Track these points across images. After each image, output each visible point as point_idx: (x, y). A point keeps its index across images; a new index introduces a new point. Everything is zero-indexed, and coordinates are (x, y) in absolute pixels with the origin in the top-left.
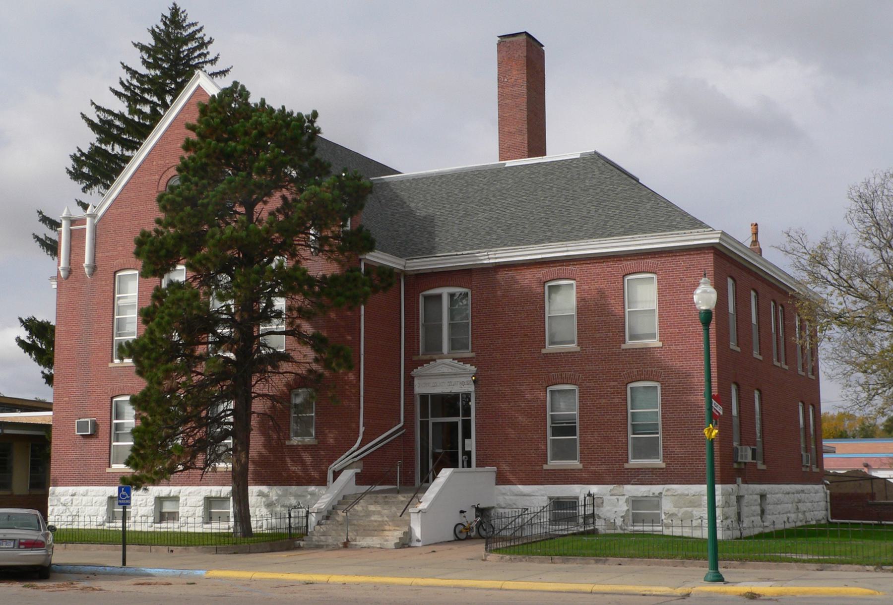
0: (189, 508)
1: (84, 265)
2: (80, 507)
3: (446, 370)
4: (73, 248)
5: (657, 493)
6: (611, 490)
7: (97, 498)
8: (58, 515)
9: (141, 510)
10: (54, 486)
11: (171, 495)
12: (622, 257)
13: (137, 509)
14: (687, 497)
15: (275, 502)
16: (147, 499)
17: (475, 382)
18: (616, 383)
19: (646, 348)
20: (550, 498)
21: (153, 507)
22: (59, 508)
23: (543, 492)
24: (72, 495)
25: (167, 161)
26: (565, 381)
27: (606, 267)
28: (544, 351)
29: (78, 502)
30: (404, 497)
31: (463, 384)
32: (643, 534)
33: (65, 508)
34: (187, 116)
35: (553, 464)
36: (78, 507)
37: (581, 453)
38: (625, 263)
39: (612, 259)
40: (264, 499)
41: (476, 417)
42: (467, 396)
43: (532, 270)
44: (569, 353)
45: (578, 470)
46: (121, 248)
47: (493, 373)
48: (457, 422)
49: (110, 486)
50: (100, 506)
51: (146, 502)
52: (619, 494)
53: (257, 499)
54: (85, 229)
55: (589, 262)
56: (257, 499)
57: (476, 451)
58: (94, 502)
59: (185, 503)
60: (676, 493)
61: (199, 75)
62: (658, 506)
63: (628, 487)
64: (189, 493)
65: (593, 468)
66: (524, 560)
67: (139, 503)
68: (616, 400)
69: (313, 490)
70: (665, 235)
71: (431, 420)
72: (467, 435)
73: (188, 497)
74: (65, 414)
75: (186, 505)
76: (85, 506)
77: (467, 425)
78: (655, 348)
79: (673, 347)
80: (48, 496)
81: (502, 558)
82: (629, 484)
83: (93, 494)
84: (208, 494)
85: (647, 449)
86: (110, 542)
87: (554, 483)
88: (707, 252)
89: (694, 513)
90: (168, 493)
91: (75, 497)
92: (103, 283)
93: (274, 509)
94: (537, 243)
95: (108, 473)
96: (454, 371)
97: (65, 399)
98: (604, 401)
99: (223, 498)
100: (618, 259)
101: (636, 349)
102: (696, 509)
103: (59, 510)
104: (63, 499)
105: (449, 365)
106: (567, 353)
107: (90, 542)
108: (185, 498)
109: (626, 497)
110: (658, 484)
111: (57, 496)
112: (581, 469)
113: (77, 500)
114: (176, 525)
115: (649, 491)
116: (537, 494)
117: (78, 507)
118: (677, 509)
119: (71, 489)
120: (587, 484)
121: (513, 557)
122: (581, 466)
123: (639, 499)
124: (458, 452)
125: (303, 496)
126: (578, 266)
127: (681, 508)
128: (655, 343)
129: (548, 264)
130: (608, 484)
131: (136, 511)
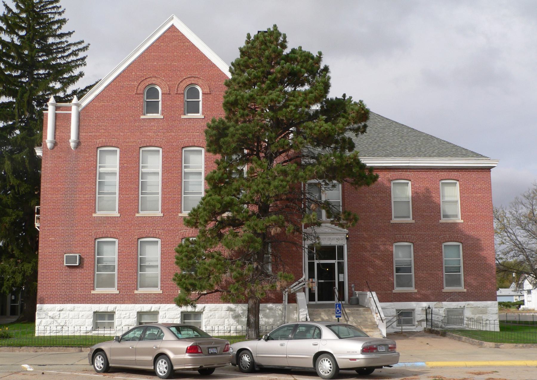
0: (168, 319)
1: (70, 141)
2: (67, 320)
3: (327, 230)
4: (57, 127)
5: (462, 306)
6: (435, 305)
7: (83, 312)
8: (46, 326)
9: (125, 321)
10: (40, 304)
11: (152, 310)
12: (439, 170)
13: (121, 321)
14: (479, 308)
15: (241, 314)
16: (130, 313)
17: (347, 239)
18: (436, 243)
19: (454, 223)
20: (397, 310)
21: (136, 319)
22: (47, 320)
23: (393, 307)
24: (60, 311)
25: (145, 73)
26: (406, 240)
27: (431, 175)
28: (392, 222)
29: (65, 315)
30: (350, 310)
31: (338, 239)
32: (454, 330)
33: (53, 320)
34: (162, 44)
35: (397, 290)
36: (65, 320)
37: (416, 283)
38: (441, 173)
39: (433, 170)
40: (231, 313)
41: (348, 260)
42: (341, 248)
43: (383, 172)
44: (408, 223)
45: (414, 293)
46: (103, 131)
47: (359, 233)
48: (334, 263)
49: (95, 304)
50: (86, 318)
51: (130, 315)
52: (439, 307)
53: (226, 313)
54: (70, 115)
55: (419, 171)
56: (226, 313)
57: (348, 281)
58: (80, 316)
59: (164, 316)
60: (473, 306)
61: (173, 18)
62: (462, 313)
63: (445, 303)
64: (168, 309)
65: (423, 292)
66: (532, 347)
67: (122, 316)
68: (437, 252)
69: (271, 306)
70: (479, 159)
71: (316, 262)
72: (341, 271)
73: (167, 312)
74: (51, 250)
75: (165, 317)
76: (72, 318)
77: (341, 265)
78: (459, 223)
79: (469, 223)
80: (35, 311)
81: (516, 346)
82: (445, 301)
83: (80, 309)
84: (139, 310)
85: (455, 281)
86: (59, 345)
87: (400, 301)
88: (487, 171)
89: (484, 317)
90: (149, 309)
91: (62, 312)
92: (87, 155)
93: (240, 319)
94: (386, 156)
95: (92, 294)
96: (340, 232)
97: (50, 239)
98: (429, 253)
99: (196, 312)
100: (437, 170)
101: (448, 223)
102: (484, 315)
103: (47, 322)
104: (50, 314)
105: (329, 227)
106: (406, 223)
107: (68, 346)
108: (165, 312)
109: (444, 309)
110: (462, 301)
111: (44, 311)
112: (416, 293)
113: (64, 314)
114: (112, 332)
115: (458, 305)
116: (389, 308)
117: (65, 320)
118: (474, 315)
119: (58, 306)
120: (420, 301)
121: (525, 345)
122: (416, 291)
123: (451, 310)
124: (335, 282)
125: (264, 310)
126: (412, 173)
127: (476, 314)
128: (459, 220)
129: (394, 170)
130: (432, 301)
131: (120, 322)
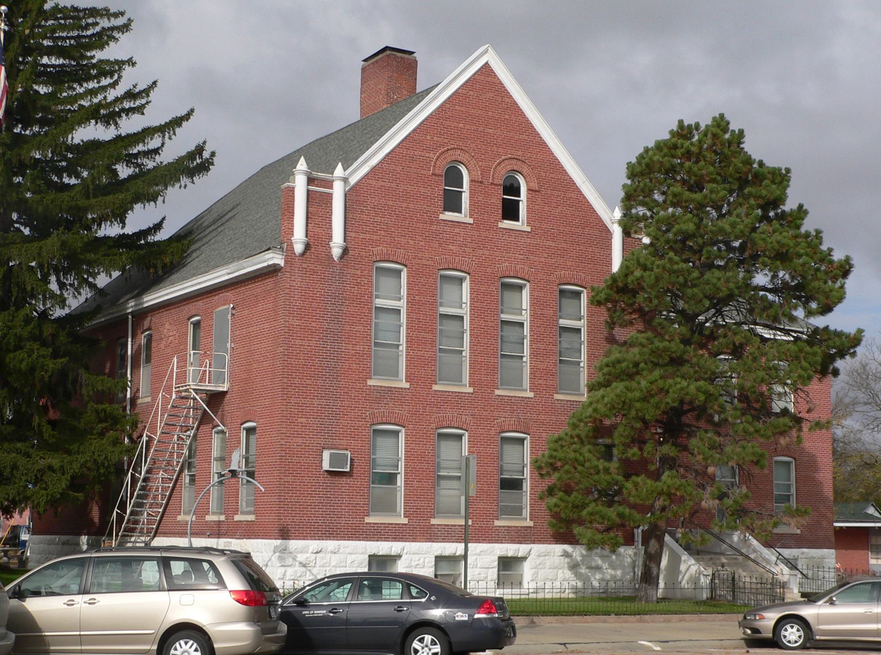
2: (328, 569)
7: (353, 556)
10: (283, 539)
16: (425, 558)
22: (296, 568)
24: (317, 553)
25: (446, 141)
29: (325, 561)
33: (304, 569)
34: (471, 93)
40: (567, 560)
49: (370, 540)
50: (358, 566)
51: (424, 562)
58: (349, 562)
74: (300, 440)
83: (348, 550)
92: (359, 272)
95: (367, 523)
97: (300, 420)
103: (296, 572)
104: (301, 558)
111: (291, 553)
113: (323, 558)
117: (324, 569)
119: (314, 545)
